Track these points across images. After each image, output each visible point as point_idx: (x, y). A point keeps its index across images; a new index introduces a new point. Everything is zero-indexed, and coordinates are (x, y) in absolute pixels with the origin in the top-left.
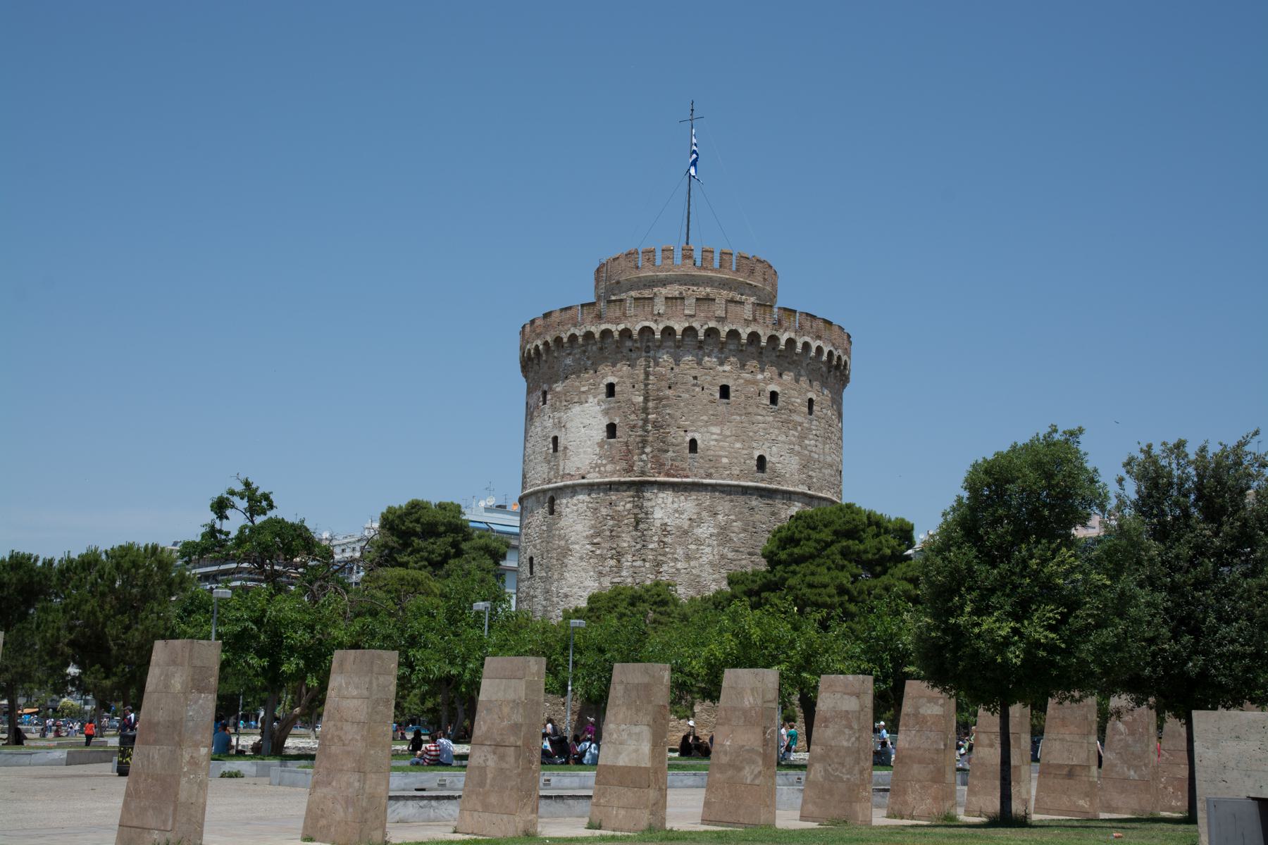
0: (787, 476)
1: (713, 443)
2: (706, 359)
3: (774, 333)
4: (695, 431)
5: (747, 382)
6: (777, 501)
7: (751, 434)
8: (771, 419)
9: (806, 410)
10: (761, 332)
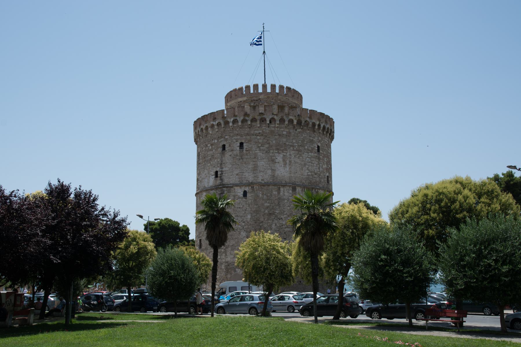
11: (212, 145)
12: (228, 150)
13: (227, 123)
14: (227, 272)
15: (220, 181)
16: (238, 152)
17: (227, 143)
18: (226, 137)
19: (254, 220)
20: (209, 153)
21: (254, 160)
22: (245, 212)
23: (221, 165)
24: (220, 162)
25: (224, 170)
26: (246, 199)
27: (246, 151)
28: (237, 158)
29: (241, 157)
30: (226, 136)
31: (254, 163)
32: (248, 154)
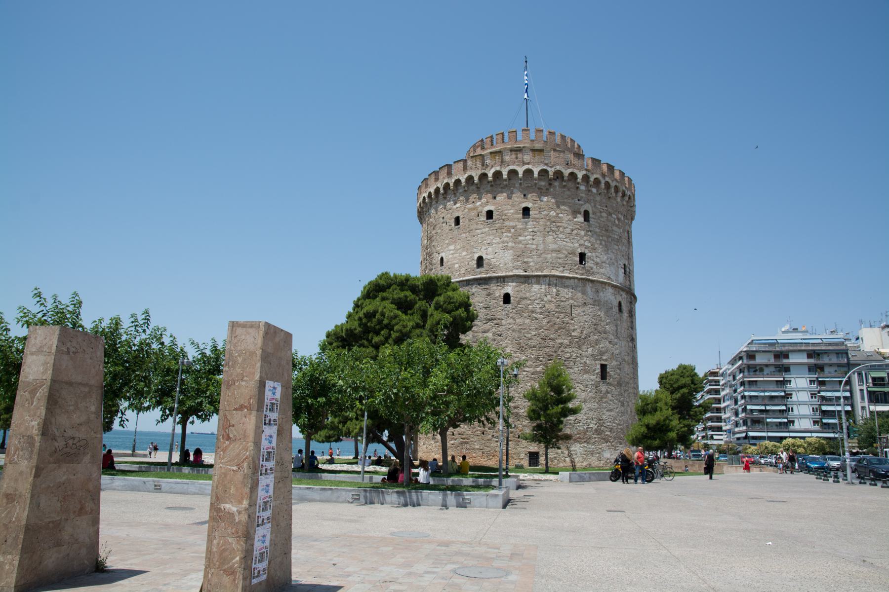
0: (501, 266)
1: (451, 256)
2: (448, 203)
3: (483, 171)
4: (442, 252)
5: (470, 210)
6: (492, 285)
7: (472, 243)
8: (487, 229)
10: (474, 175)
11: (619, 219)
20: (615, 228)
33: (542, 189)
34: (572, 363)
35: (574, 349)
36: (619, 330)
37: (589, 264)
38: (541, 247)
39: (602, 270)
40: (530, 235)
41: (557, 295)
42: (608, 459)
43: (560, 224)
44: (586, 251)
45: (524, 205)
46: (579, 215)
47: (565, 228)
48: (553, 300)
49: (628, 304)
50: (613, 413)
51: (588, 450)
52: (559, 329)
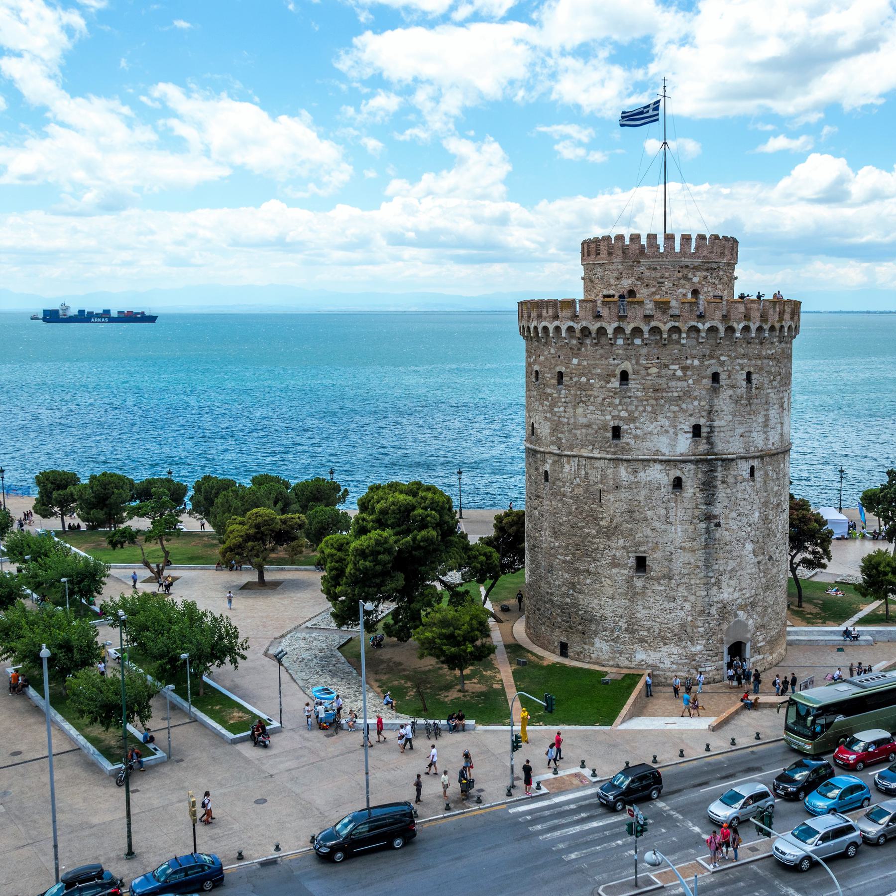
9: (555, 382)
11: (684, 368)
12: (726, 385)
13: (730, 330)
14: (721, 620)
15: (706, 447)
16: (744, 391)
17: (724, 371)
18: (722, 358)
19: (763, 520)
20: (673, 384)
21: (765, 407)
22: (752, 507)
23: (710, 412)
24: (707, 407)
25: (716, 424)
26: (753, 481)
27: (757, 389)
28: (742, 402)
29: (749, 401)
30: (722, 355)
31: (765, 413)
32: (759, 396)
33: (574, 349)
34: (599, 555)
35: (601, 540)
36: (672, 513)
37: (625, 439)
38: (572, 421)
39: (648, 444)
40: (562, 406)
41: (586, 478)
42: (643, 660)
43: (590, 393)
44: (621, 424)
45: (558, 369)
46: (613, 380)
47: (595, 397)
48: (583, 484)
49: (700, 476)
50: (654, 611)
51: (615, 649)
52: (588, 516)
